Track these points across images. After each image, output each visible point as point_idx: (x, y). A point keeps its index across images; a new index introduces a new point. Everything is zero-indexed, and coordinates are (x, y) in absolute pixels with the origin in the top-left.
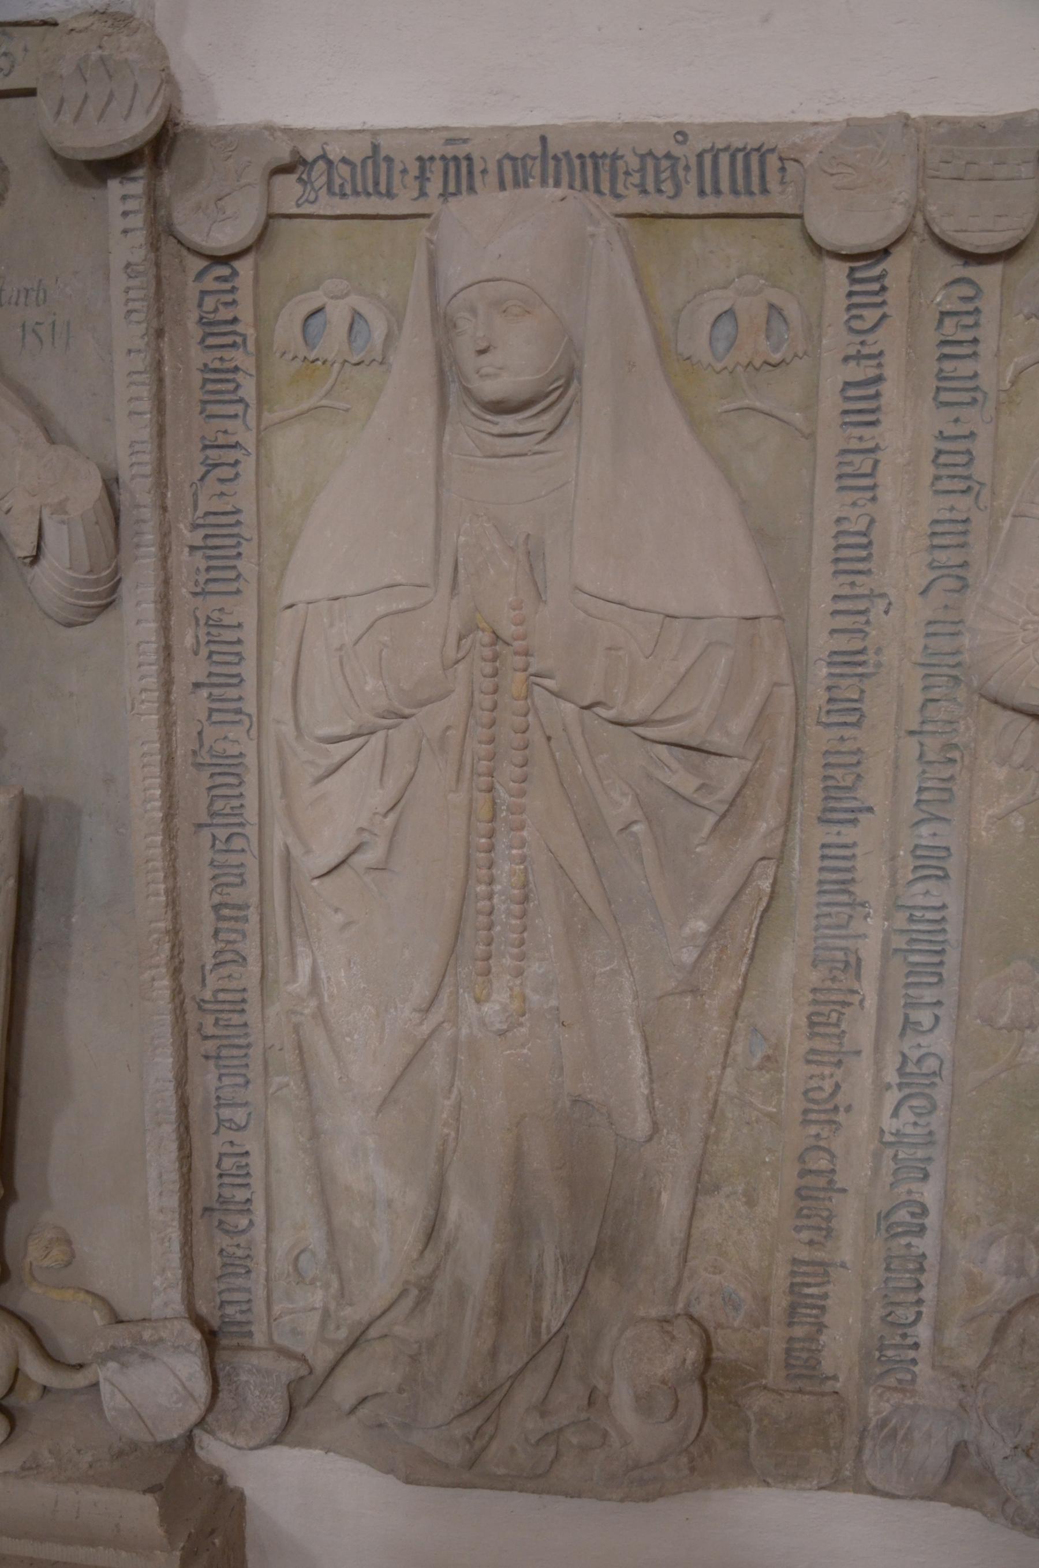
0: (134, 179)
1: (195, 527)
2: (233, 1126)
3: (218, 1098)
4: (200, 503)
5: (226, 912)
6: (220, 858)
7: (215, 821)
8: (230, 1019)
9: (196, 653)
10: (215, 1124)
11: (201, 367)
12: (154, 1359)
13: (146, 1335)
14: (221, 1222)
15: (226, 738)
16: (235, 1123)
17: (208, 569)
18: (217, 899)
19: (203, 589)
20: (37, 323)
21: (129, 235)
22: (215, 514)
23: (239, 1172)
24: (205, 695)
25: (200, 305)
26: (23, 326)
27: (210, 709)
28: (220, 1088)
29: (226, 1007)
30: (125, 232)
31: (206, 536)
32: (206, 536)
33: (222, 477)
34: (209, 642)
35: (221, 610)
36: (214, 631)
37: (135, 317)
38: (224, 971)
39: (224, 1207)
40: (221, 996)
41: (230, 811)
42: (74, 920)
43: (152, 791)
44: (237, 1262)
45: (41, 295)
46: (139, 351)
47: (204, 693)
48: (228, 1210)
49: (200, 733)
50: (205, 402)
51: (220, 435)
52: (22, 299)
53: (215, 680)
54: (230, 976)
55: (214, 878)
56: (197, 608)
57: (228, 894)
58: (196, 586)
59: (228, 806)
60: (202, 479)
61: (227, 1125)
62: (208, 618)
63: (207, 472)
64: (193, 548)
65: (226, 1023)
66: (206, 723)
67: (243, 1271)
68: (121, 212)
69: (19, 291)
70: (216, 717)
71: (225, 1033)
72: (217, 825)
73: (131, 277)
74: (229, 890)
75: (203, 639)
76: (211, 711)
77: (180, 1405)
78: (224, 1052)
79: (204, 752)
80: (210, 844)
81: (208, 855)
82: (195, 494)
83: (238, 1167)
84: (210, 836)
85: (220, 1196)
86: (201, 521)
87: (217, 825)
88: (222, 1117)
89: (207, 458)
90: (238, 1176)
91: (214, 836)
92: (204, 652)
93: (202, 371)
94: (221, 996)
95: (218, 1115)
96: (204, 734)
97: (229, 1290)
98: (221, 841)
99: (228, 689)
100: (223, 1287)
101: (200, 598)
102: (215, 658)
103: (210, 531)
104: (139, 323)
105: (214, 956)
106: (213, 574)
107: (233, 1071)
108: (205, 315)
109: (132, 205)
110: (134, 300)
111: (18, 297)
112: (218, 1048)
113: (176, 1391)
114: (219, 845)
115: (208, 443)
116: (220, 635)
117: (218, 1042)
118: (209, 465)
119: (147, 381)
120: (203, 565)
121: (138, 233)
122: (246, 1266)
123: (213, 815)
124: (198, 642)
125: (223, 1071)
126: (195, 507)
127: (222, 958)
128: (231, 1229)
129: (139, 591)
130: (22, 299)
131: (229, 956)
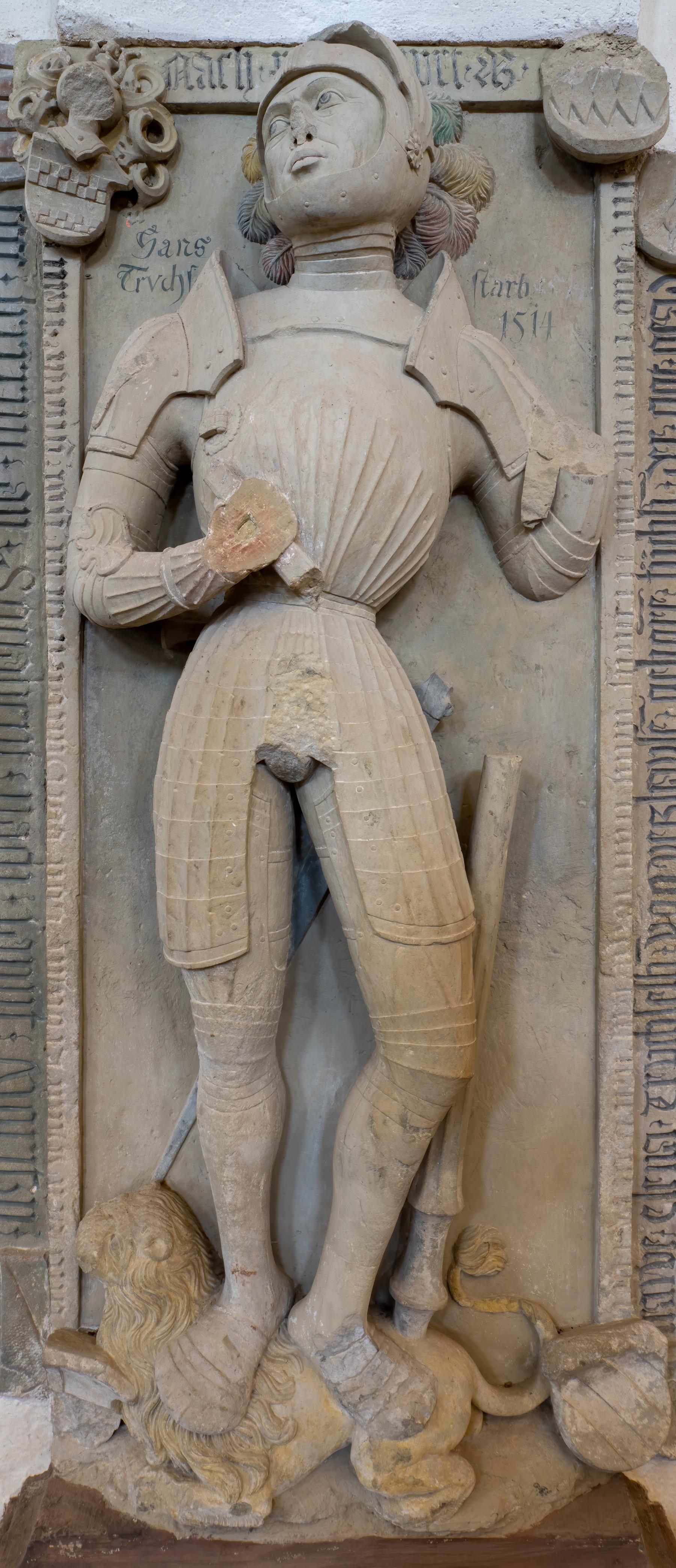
0: (625, 185)
1: (642, 513)
2: (662, 1105)
3: (648, 1075)
4: (647, 491)
5: (661, 884)
6: (659, 831)
7: (654, 795)
8: (663, 993)
9: (640, 632)
10: (644, 1103)
11: (652, 367)
12: (616, 1371)
13: (615, 1344)
14: (647, 1208)
15: (667, 713)
16: (664, 1101)
17: (654, 552)
18: (654, 871)
19: (648, 571)
20: (519, 314)
21: (619, 234)
22: (660, 502)
23: (667, 1153)
24: (648, 672)
25: (653, 313)
26: (505, 315)
27: (651, 685)
28: (649, 1065)
29: (660, 980)
30: (616, 231)
31: (653, 522)
32: (653, 522)
33: (668, 468)
34: (653, 621)
35: (666, 591)
36: (658, 611)
37: (623, 307)
38: (658, 944)
39: (650, 1192)
40: (655, 970)
41: (670, 785)
42: (524, 897)
43: (623, 761)
44: (661, 1250)
45: (524, 288)
46: (626, 339)
47: (647, 670)
48: (652, 1195)
49: (642, 709)
50: (653, 400)
51: (668, 430)
52: (505, 291)
53: (657, 658)
54: (665, 949)
55: (651, 851)
56: (642, 590)
57: (665, 866)
58: (642, 568)
59: (668, 779)
60: (650, 469)
61: (656, 1103)
62: (653, 599)
63: (654, 464)
64: (640, 533)
65: (658, 997)
66: (648, 699)
67: (666, 1259)
68: (613, 212)
69: (501, 284)
70: (658, 693)
71: (657, 1007)
72: (655, 798)
73: (619, 271)
74: (666, 862)
75: (647, 618)
76: (653, 686)
77: (646, 1421)
78: (656, 1028)
79: (645, 727)
80: (648, 817)
81: (648, 828)
82: (643, 484)
83: (665, 1147)
84: (649, 809)
85: (647, 1180)
86: (647, 508)
87: (655, 798)
88: (651, 1096)
89: (656, 450)
90: (664, 1157)
91: (652, 808)
92: (647, 631)
93: (652, 371)
94: (655, 970)
95: (647, 1093)
96: (646, 709)
97: (650, 1282)
98: (659, 814)
99: (670, 666)
100: (646, 1278)
101: (646, 580)
102: (658, 636)
103: (657, 518)
104: (626, 312)
105: (650, 930)
106: (659, 558)
107: (662, 1047)
108: (658, 322)
109: (622, 207)
110: (622, 292)
111: (501, 288)
112: (649, 1024)
113: (639, 1405)
114: (658, 818)
115: (656, 436)
116: (663, 615)
117: (648, 1018)
118: (656, 457)
119: (633, 367)
120: (649, 548)
121: (628, 232)
122: (671, 1255)
123: (655, 787)
124: (642, 622)
125: (654, 1047)
126: (643, 494)
127: (656, 931)
128: (656, 1214)
129: (617, 564)
130: (505, 291)
131: (665, 929)
